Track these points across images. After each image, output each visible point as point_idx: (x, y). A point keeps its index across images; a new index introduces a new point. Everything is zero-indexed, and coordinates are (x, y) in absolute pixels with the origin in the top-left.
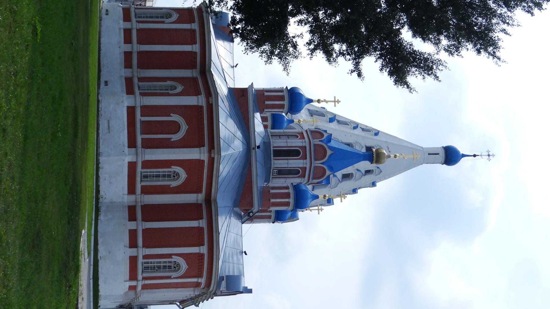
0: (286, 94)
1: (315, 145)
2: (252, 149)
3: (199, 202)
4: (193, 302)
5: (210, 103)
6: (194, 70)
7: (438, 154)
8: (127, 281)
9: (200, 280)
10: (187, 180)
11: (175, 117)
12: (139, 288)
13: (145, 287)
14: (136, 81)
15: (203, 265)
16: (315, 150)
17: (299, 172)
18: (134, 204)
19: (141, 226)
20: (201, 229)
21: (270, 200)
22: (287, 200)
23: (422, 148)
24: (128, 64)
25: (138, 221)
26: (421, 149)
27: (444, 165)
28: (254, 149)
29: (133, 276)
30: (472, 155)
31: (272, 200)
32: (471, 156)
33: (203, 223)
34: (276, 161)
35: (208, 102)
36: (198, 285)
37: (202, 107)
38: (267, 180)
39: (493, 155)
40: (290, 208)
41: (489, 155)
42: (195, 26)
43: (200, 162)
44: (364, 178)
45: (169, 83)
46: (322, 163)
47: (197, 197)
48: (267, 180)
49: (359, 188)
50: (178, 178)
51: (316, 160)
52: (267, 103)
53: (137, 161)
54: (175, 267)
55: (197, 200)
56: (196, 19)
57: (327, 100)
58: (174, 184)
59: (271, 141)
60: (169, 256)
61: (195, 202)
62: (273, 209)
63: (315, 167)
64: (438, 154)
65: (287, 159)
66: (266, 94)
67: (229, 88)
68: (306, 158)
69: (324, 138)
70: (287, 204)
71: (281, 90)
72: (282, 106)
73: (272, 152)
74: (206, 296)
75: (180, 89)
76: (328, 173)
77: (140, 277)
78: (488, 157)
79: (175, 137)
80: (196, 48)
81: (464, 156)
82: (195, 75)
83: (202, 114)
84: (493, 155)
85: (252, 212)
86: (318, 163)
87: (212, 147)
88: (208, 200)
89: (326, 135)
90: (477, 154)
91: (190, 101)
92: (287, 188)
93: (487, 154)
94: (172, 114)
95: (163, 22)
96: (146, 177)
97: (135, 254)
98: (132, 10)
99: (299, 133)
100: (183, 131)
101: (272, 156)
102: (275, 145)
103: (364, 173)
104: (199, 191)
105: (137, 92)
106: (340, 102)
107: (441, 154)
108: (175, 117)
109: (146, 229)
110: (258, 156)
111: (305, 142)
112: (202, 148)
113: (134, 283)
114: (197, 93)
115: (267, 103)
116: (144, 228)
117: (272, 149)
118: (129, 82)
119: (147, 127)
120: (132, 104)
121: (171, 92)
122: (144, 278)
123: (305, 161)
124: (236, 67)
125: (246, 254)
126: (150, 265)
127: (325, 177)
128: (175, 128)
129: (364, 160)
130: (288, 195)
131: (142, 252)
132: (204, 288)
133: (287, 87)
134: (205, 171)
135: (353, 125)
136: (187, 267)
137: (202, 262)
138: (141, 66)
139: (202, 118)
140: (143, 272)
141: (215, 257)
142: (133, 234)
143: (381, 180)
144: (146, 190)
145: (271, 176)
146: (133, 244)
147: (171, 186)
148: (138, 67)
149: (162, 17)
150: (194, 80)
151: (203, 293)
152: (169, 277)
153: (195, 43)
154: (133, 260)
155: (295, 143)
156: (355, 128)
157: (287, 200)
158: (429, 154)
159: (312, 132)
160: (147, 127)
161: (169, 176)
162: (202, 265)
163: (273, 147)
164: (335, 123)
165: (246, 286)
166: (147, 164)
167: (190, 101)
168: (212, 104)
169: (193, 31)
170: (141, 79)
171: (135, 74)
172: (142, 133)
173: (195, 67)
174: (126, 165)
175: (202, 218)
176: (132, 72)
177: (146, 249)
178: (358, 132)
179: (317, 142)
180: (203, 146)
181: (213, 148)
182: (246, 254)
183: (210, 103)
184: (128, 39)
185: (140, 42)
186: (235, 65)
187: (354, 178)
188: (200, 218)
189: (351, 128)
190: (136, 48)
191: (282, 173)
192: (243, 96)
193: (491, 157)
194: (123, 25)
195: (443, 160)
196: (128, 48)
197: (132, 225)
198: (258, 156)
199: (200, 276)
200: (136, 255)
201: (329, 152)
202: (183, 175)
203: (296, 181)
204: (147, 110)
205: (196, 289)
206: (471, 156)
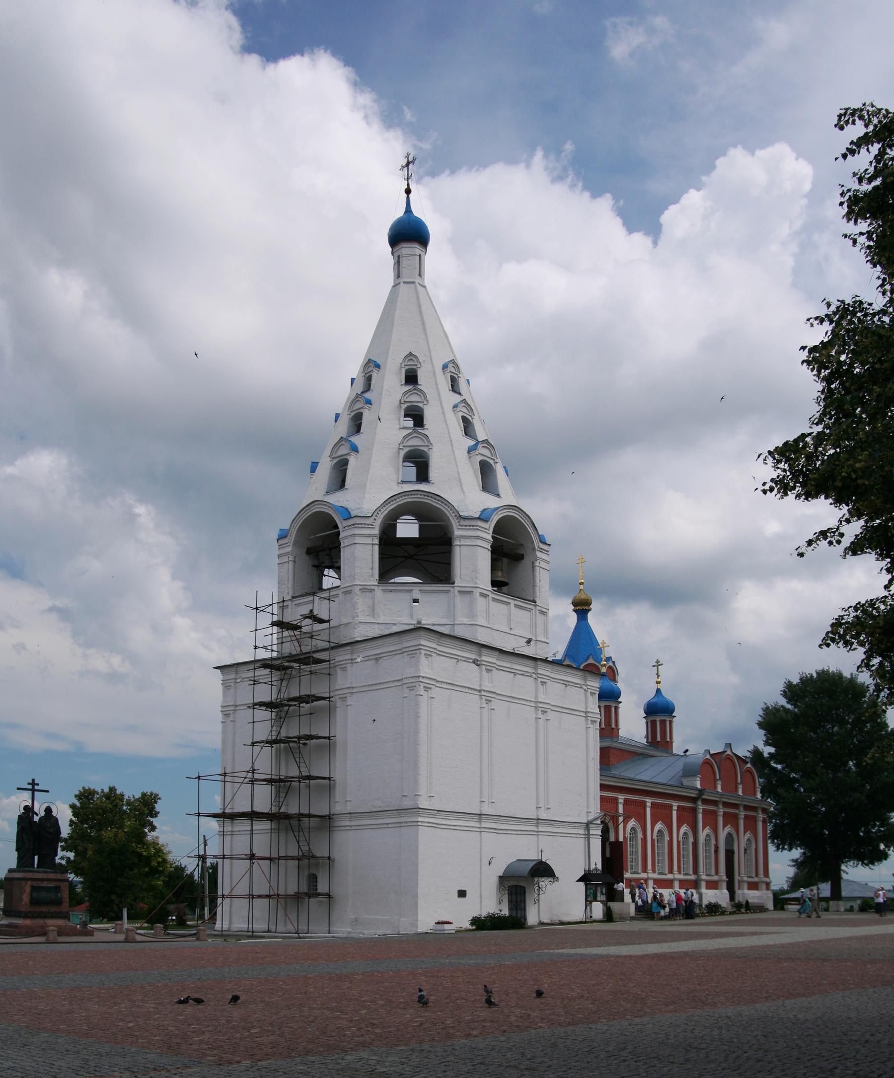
32: (408, 198)
41: (408, 164)
81: (408, 210)
90: (406, 187)
206: (408, 198)
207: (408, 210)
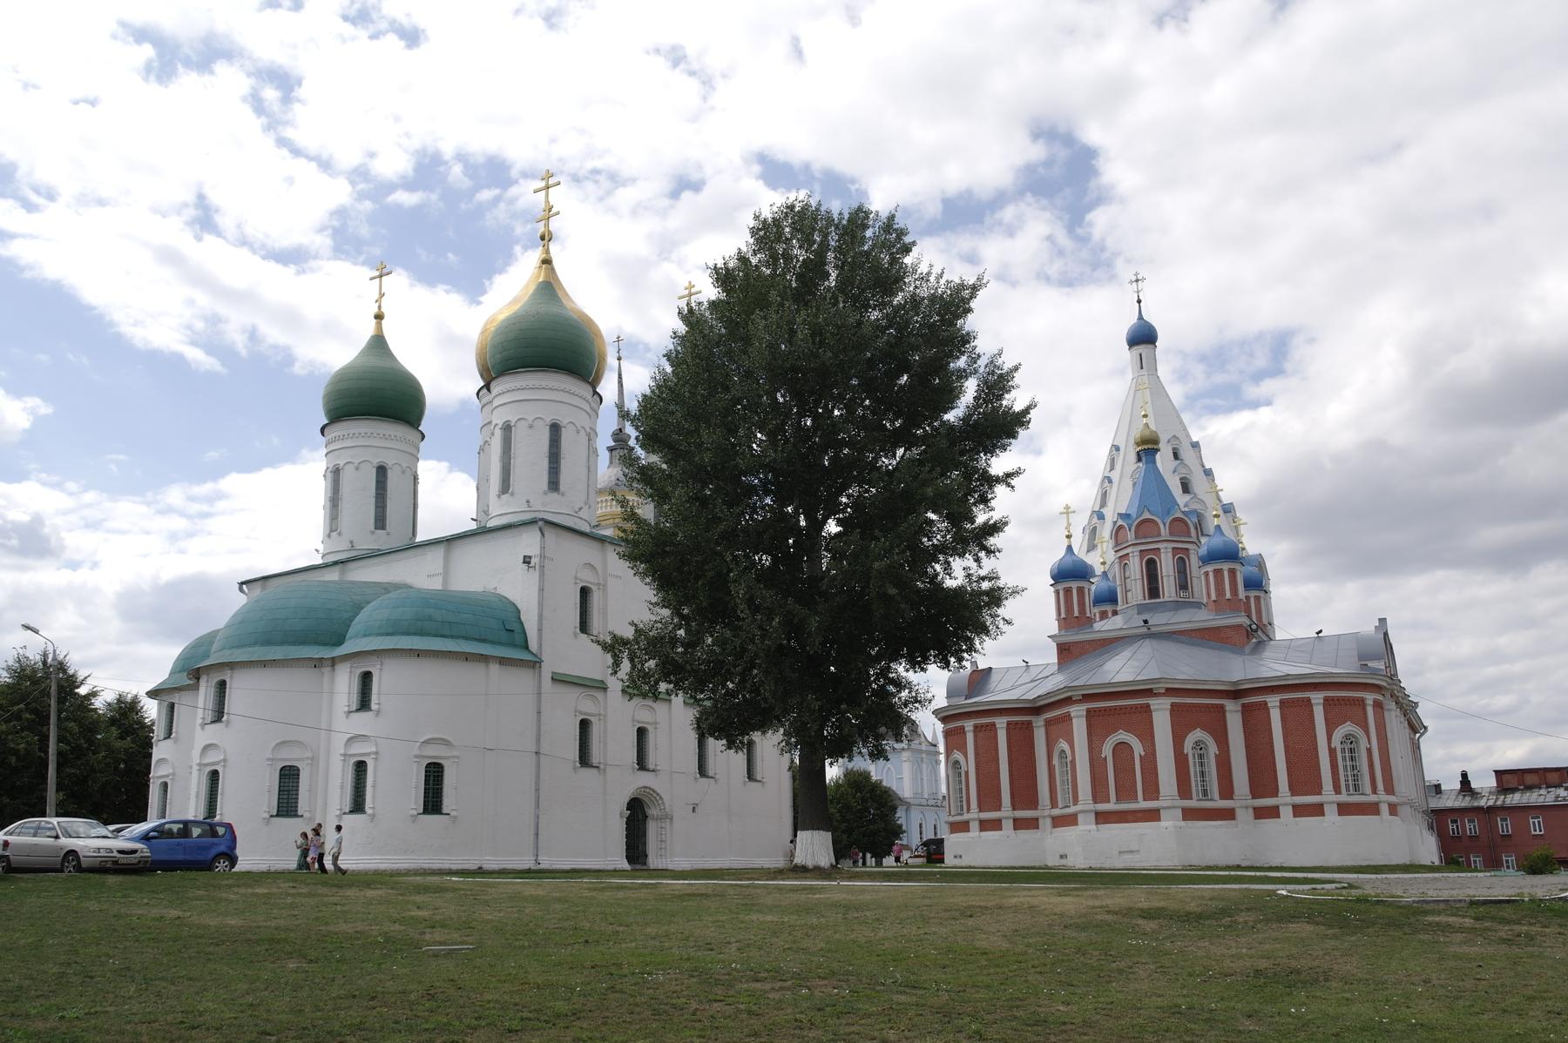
0: (1061, 587)
1: (1136, 538)
2: (1149, 632)
4: (1410, 711)
5: (1081, 698)
6: (1034, 725)
7: (1141, 355)
9: (1370, 702)
10: (1205, 728)
12: (1392, 799)
13: (1390, 789)
14: (1056, 812)
15: (1344, 699)
16: (1145, 537)
17: (1180, 558)
18: (1251, 811)
19: (1285, 798)
23: (1133, 379)
24: (1033, 824)
25: (1278, 803)
26: (1135, 380)
28: (1149, 629)
29: (1372, 809)
31: (1228, 596)
32: (1140, 306)
33: (1273, 701)
35: (1079, 701)
36: (1378, 705)
37: (1088, 711)
39: (1136, 274)
40: (1237, 567)
41: (1137, 281)
42: (969, 725)
43: (1175, 708)
44: (1187, 461)
45: (1056, 761)
46: (1165, 525)
47: (1231, 711)
48: (1198, 605)
49: (1203, 466)
50: (1204, 743)
51: (1159, 535)
53: (1178, 807)
55: (1236, 711)
56: (959, 724)
57: (1066, 525)
58: (1213, 749)
59: (1134, 603)
60: (1332, 752)
61: (1240, 714)
62: (1242, 594)
63: (1171, 534)
64: (1141, 355)
65: (1162, 578)
66: (1063, 616)
67: (1059, 669)
69: (1124, 524)
70: (1232, 572)
71: (1057, 592)
72: (1081, 590)
73: (1153, 601)
74: (1398, 691)
75: (1064, 745)
77: (1373, 798)
78: (1140, 282)
79: (1138, 748)
80: (1001, 723)
81: (1140, 317)
82: (1043, 723)
83: (1100, 710)
85: (1250, 626)
86: (1164, 531)
87: (1149, 693)
88: (1235, 694)
89: (1120, 522)
91: (1079, 727)
92: (1207, 574)
93: (1135, 284)
94: (1103, 756)
96: (1205, 793)
97: (1335, 807)
98: (951, 819)
99: (1120, 563)
100: (1128, 738)
101: (1158, 600)
103: (1179, 462)
104: (1221, 708)
105: (1073, 809)
106: (1067, 505)
107: (1140, 351)
108: (1107, 750)
109: (1290, 790)
110: (1159, 620)
111: (1133, 552)
113: (1384, 809)
114: (1067, 718)
115: (1076, 614)
116: (1289, 794)
118: (1059, 822)
119: (1125, 792)
120: (1092, 817)
121: (1070, 758)
122: (1374, 791)
123: (1162, 550)
125: (1321, 631)
126: (1350, 783)
128: (1122, 749)
129: (1154, 462)
130: (1218, 572)
131: (1328, 796)
132: (1383, 695)
133: (1051, 585)
135: (1107, 484)
136: (1349, 723)
138: (1033, 803)
139: (1105, 709)
140: (1362, 794)
141: (1328, 680)
142: (1299, 811)
143: (1188, 436)
144: (1227, 791)
145: (1191, 600)
146: (1318, 810)
147: (1217, 752)
148: (1036, 808)
149: (960, 774)
150: (1048, 723)
151: (1392, 696)
152: (1369, 751)
153: (993, 725)
154: (1344, 809)
155: (1136, 567)
156: (1110, 481)
158: (1142, 368)
159: (1117, 544)
161: (1201, 756)
162: (1217, 707)
163: (1145, 599)
164: (1104, 511)
165: (1374, 629)
166: (1184, 790)
168: (1083, 695)
169: (976, 728)
170: (1054, 804)
171: (1047, 813)
172: (1135, 799)
173: (1029, 723)
174: (1190, 823)
175: (1266, 703)
176: (1044, 817)
177: (1324, 789)
178: (1115, 476)
179: (1131, 536)
180: (1148, 706)
181: (1150, 690)
182: (1321, 631)
183: (1081, 698)
184: (995, 825)
185: (999, 808)
187: (1188, 476)
189: (1111, 487)
190: (1006, 812)
191: (1183, 585)
193: (1140, 277)
194: (974, 832)
195: (1151, 346)
196: (1008, 825)
197: (1286, 812)
198: (1159, 620)
200: (1336, 805)
201: (1147, 515)
202: (1197, 734)
203: (1194, 561)
204: (1099, 793)
206: (1140, 306)
207: (1140, 317)
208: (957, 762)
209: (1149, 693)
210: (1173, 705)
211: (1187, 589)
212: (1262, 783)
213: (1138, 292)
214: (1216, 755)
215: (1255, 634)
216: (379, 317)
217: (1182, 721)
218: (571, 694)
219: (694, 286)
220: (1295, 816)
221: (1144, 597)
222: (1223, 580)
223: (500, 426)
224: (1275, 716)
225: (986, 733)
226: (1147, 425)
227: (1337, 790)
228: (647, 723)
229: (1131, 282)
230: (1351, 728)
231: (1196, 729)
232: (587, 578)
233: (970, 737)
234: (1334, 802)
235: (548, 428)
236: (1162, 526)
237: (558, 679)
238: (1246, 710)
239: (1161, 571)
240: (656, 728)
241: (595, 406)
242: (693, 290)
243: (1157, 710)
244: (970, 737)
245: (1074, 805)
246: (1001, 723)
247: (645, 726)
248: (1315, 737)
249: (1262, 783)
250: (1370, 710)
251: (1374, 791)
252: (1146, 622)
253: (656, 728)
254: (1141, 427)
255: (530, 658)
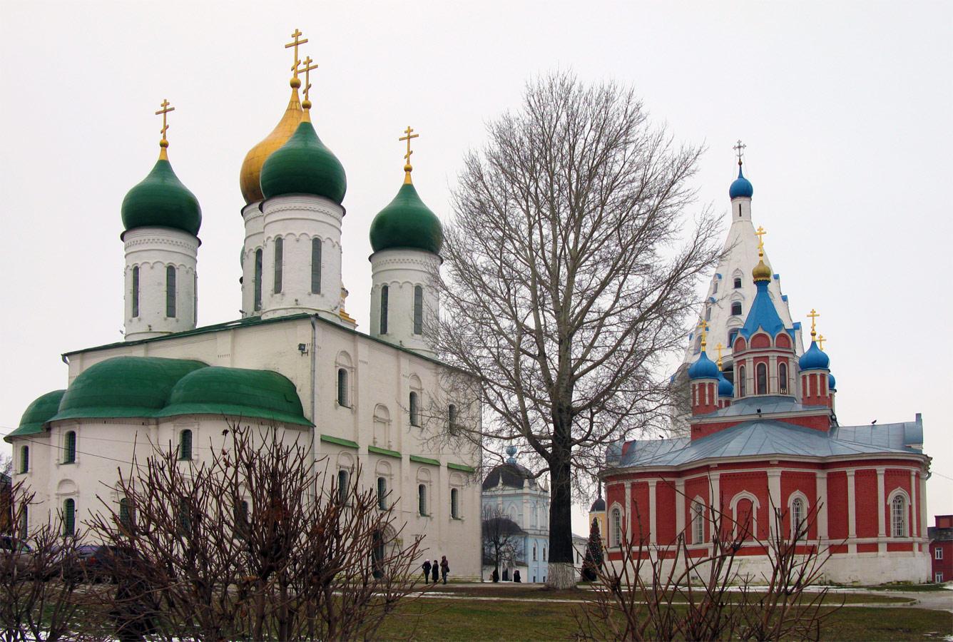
1: (752, 348)
3: (825, 476)
7: (740, 205)
8: (914, 554)
10: (801, 490)
11: (733, 505)
12: (920, 540)
19: (853, 539)
20: (857, 474)
21: (819, 397)
22: (818, 377)
27: (752, 197)
28: (760, 416)
30: (739, 166)
31: (819, 394)
32: (741, 168)
33: (851, 472)
34: (771, 391)
35: (716, 469)
37: (722, 476)
38: (792, 399)
39: (739, 142)
41: (739, 147)
45: (692, 512)
51: (769, 346)
52: (707, 402)
54: (899, 502)
55: (823, 478)
60: (887, 508)
63: (777, 346)
64: (740, 205)
65: (769, 378)
67: (692, 444)
68: (768, 357)
69: (743, 337)
75: (699, 499)
76: (783, 332)
77: (910, 539)
78: (742, 149)
80: (652, 482)
81: (741, 176)
82: (683, 483)
84: (739, 142)
86: (773, 343)
87: (766, 464)
88: (823, 466)
91: (715, 486)
92: (804, 377)
93: (737, 150)
94: (730, 508)
95: (624, 518)
101: (765, 395)
102: (753, 392)
104: (813, 477)
107: (740, 202)
108: (733, 505)
110: (769, 410)
112: (768, 474)
113: (916, 546)
114: (705, 481)
115: (707, 402)
117: (757, 396)
122: (911, 535)
123: (770, 358)
124: (663, 437)
125: (875, 421)
127: (788, 335)
128: (745, 506)
129: (766, 290)
130: (813, 377)
131: (882, 538)
134: (793, 470)
136: (899, 488)
137: (894, 472)
142: (862, 548)
146: (874, 548)
149: (618, 519)
152: (910, 507)
153: (647, 484)
154: (892, 547)
157: (818, 377)
158: (740, 215)
160: (746, 534)
161: (797, 510)
167: (715, 486)
168: (718, 464)
173: (673, 483)
175: (845, 473)
180: (766, 473)
181: (768, 462)
182: (875, 421)
186: (661, 439)
188: (844, 475)
191: (783, 385)
192: (700, 429)
193: (742, 144)
195: (747, 199)
197: (852, 549)
198: (769, 410)
199: (909, 473)
200: (886, 545)
201: (760, 331)
202: (797, 494)
203: (792, 369)
205: (922, 477)
206: (741, 168)
207: (741, 176)
208: (616, 510)
209: (766, 464)
210: (783, 473)
211: (786, 387)
212: (838, 527)
213: (740, 156)
214: (808, 509)
215: (827, 424)
216: (164, 145)
217: (789, 484)
218: (334, 452)
219: (412, 131)
220: (858, 552)
221: (755, 392)
222: (816, 383)
223: (273, 239)
224: (851, 482)
225: (640, 490)
226: (761, 262)
227: (888, 534)
228: (385, 475)
229: (735, 148)
230: (900, 492)
231: (795, 490)
232: (344, 361)
233: (628, 492)
234: (885, 542)
235: (311, 242)
236: (771, 340)
237: (326, 441)
238: (830, 478)
239: (769, 373)
240: (391, 479)
241: (336, 224)
242: (412, 134)
243: (771, 476)
244: (628, 492)
245: (705, 542)
246: (652, 482)
247: (384, 477)
248: (877, 497)
249: (838, 527)
250: (913, 479)
251: (911, 535)
252: (759, 411)
253: (391, 479)
254: (758, 263)
255: (306, 423)
